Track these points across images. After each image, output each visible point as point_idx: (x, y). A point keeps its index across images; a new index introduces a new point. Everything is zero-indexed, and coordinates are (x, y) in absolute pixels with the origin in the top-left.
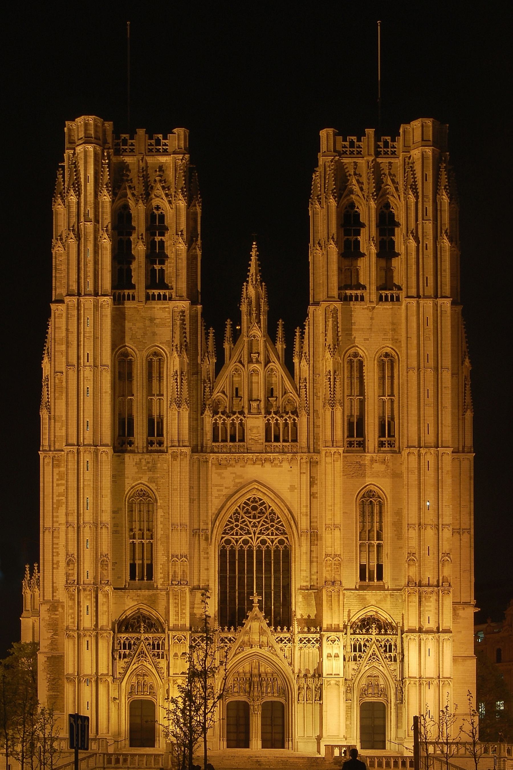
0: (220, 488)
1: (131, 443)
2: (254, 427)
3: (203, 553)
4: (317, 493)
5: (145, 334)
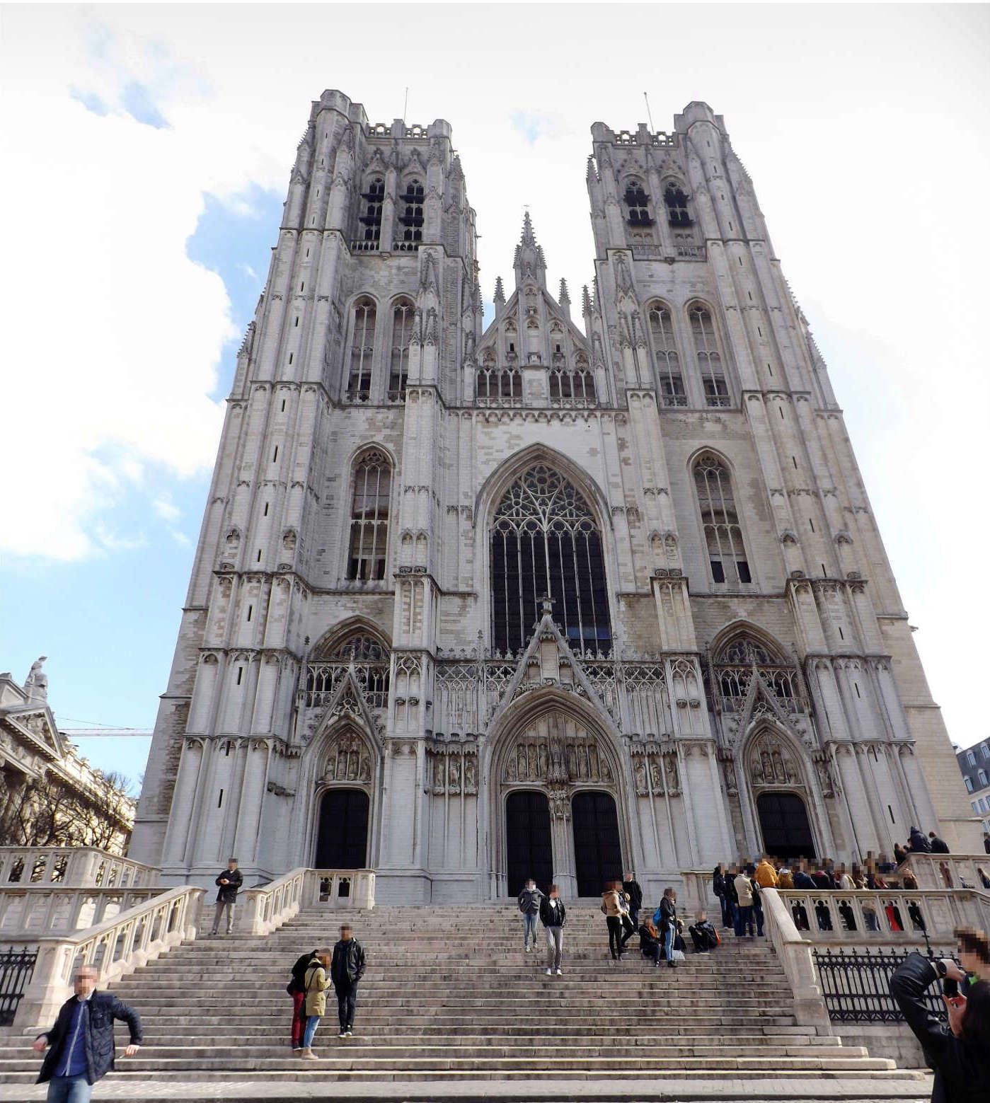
1: (365, 398)
4: (629, 459)
5: (390, 282)
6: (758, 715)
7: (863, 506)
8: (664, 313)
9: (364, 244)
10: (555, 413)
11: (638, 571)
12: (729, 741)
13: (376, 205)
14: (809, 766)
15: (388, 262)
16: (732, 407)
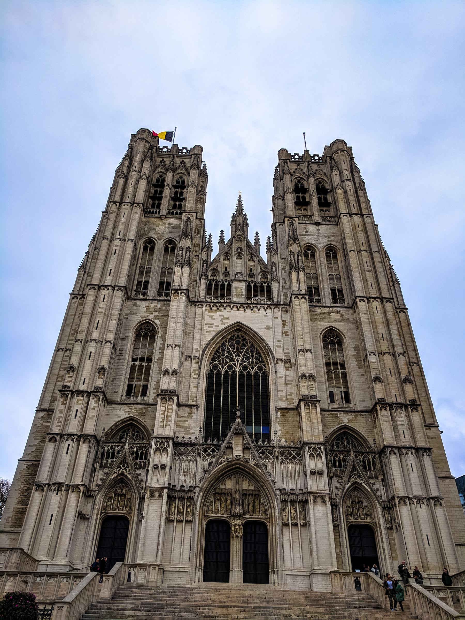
0: (211, 326)
1: (144, 294)
2: (238, 287)
3: (193, 374)
6: (353, 480)
7: (417, 362)
8: (312, 252)
9: (152, 210)
10: (249, 306)
11: (289, 395)
12: (336, 494)
13: (159, 190)
14: (379, 509)
15: (164, 221)
16: (346, 305)
